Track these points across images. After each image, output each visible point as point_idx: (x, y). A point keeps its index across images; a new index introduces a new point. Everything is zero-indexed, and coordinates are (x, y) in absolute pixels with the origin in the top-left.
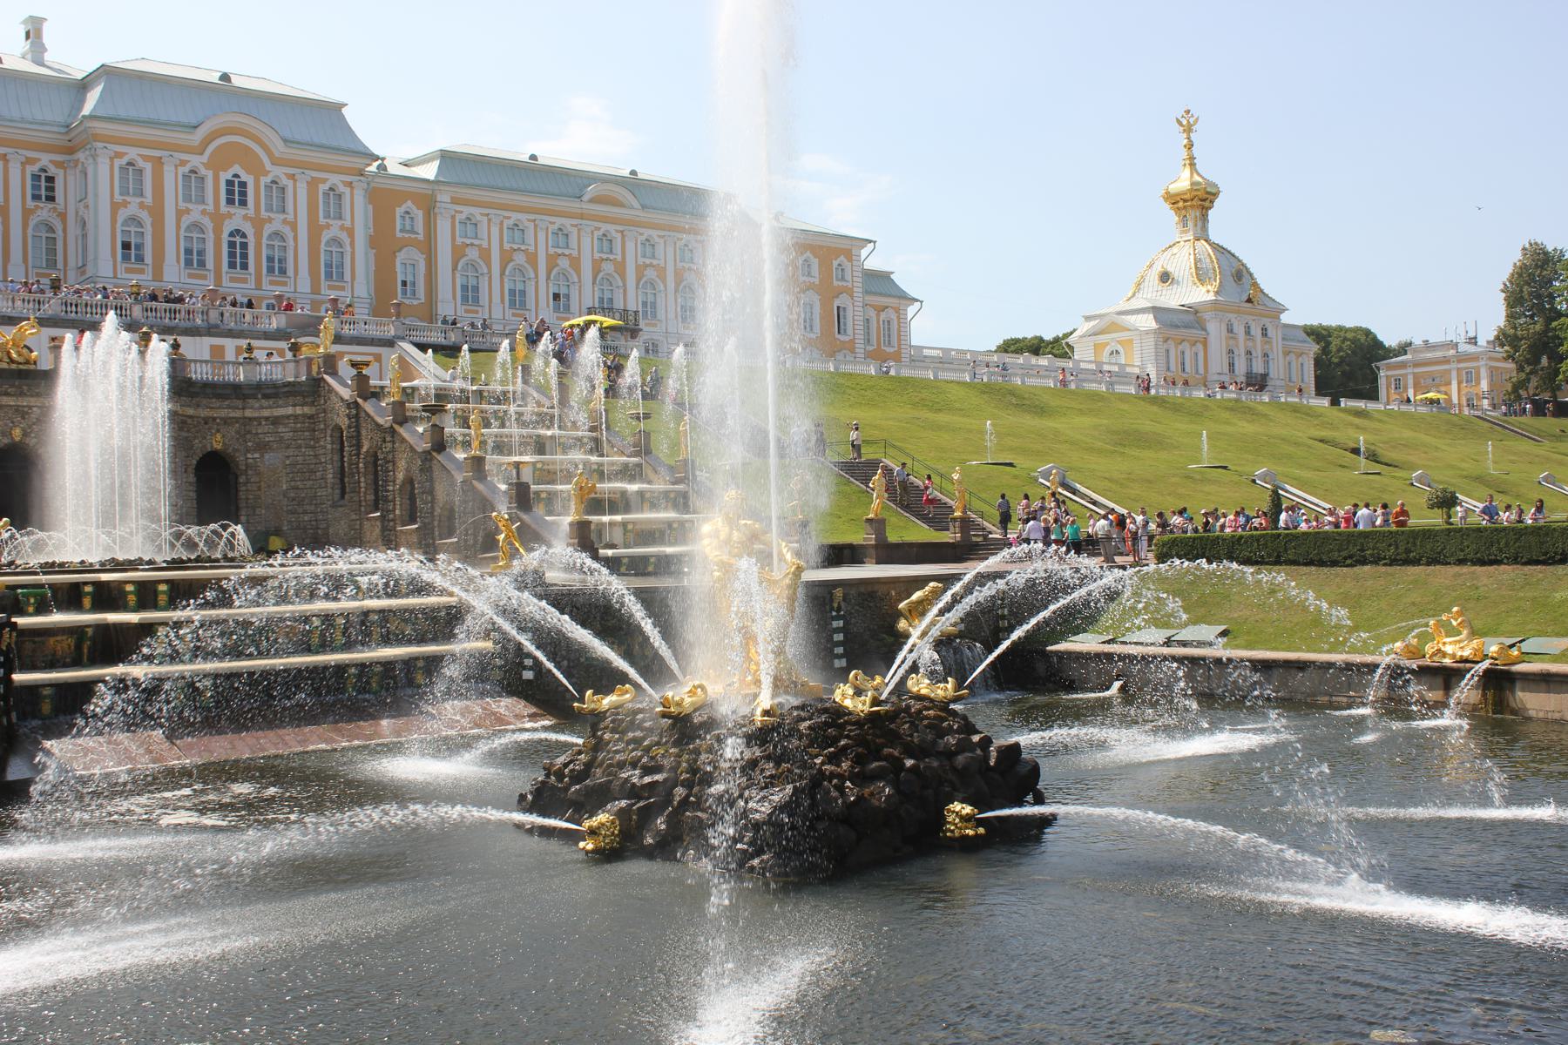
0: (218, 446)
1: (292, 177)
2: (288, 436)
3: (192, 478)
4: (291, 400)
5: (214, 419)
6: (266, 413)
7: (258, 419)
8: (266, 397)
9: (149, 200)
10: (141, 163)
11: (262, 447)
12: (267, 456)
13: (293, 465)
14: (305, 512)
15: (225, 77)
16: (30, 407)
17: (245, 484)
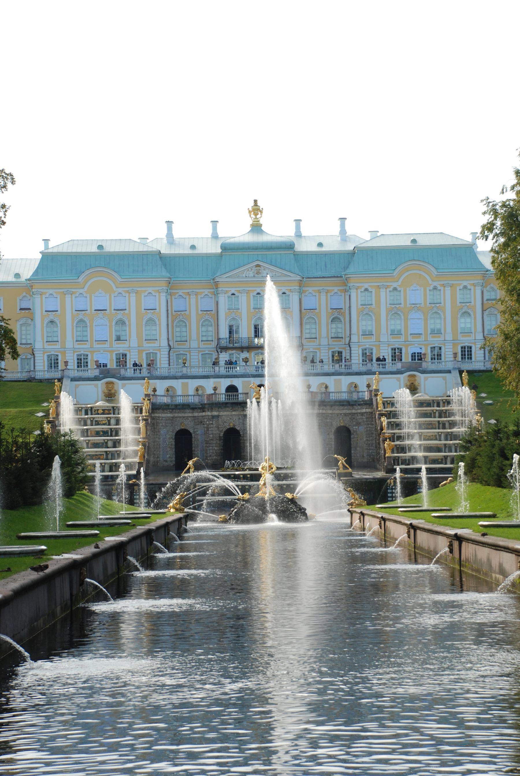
0: (342, 425)
1: (444, 286)
2: (365, 420)
3: (332, 436)
4: (365, 407)
5: (341, 414)
6: (359, 411)
7: (357, 413)
8: (359, 405)
9: (374, 306)
10: (370, 290)
11: (359, 424)
12: (360, 428)
13: (367, 431)
14: (370, 449)
15: (414, 241)
17: (353, 438)
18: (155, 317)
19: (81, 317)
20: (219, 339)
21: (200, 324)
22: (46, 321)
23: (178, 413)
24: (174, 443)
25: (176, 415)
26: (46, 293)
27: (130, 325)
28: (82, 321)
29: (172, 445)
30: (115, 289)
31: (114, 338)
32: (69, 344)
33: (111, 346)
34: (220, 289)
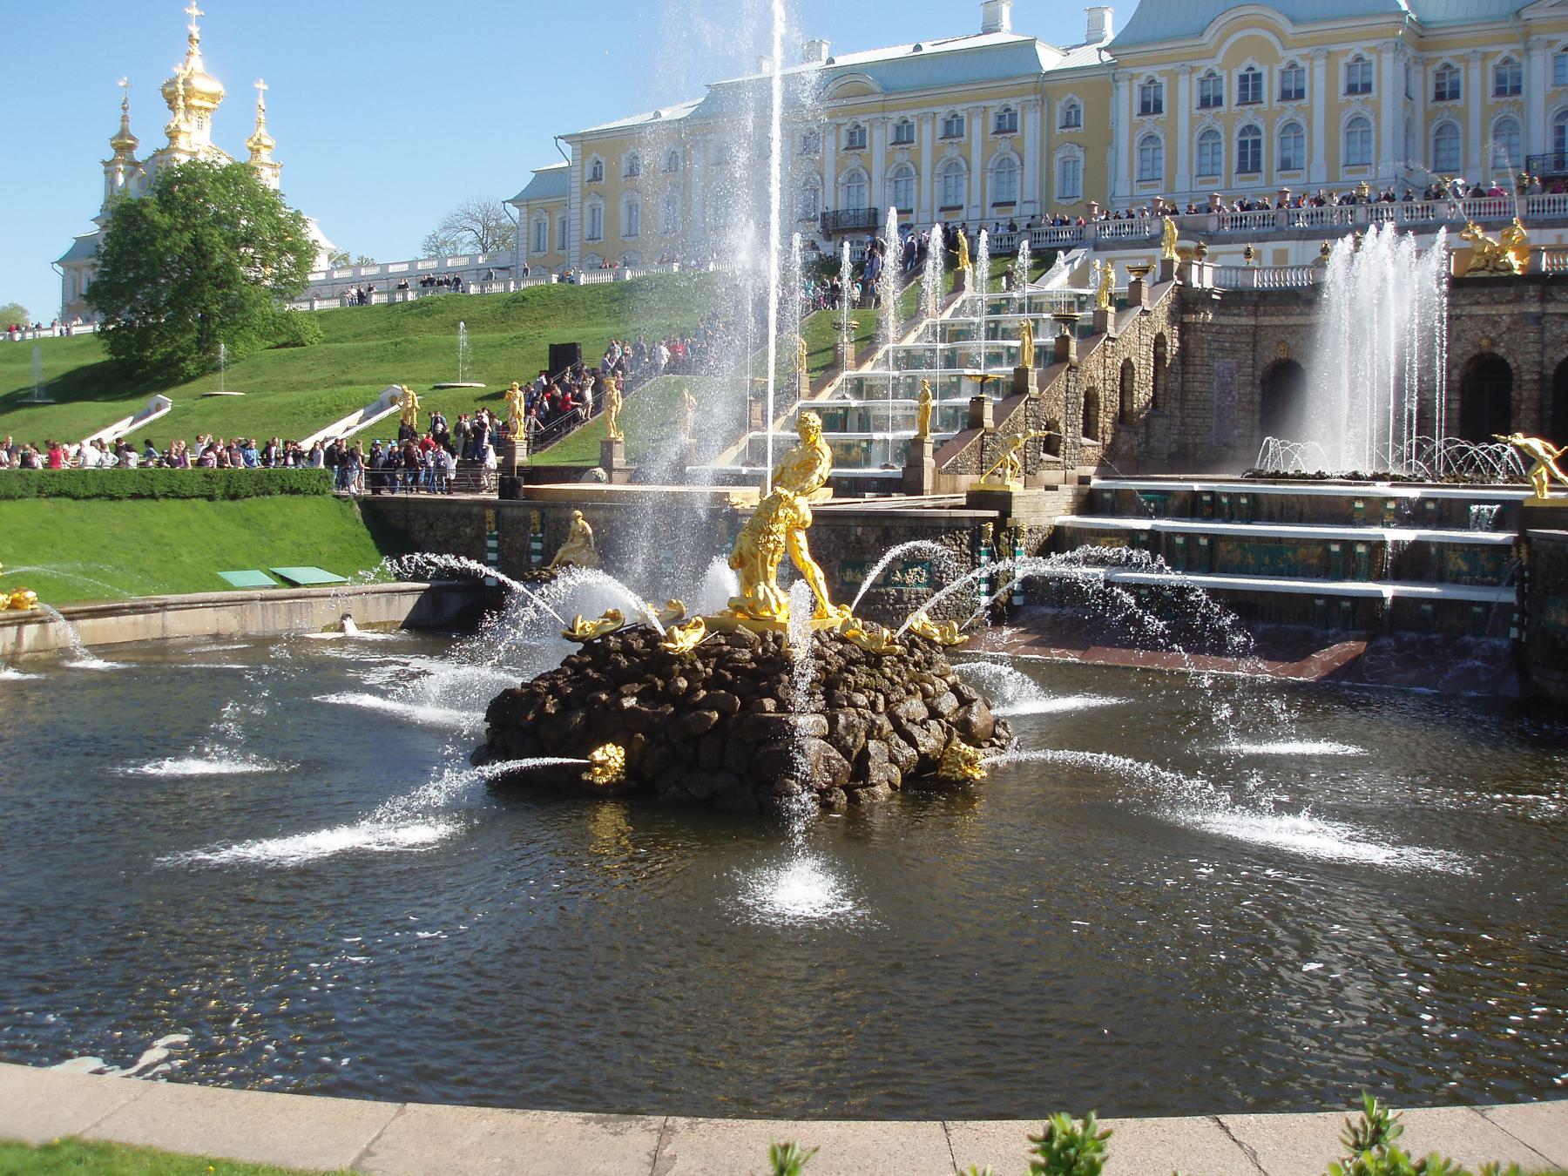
16: (1500, 316)
18: (1367, 114)
19: (1208, 121)
20: (1528, 159)
21: (1491, 128)
22: (1137, 139)
23: (1272, 314)
24: (1257, 398)
25: (1266, 321)
26: (1139, 75)
27: (1311, 132)
28: (1210, 133)
29: (1251, 402)
30: (1281, 53)
31: (1276, 164)
32: (1182, 185)
33: (1269, 183)
34: (1534, 38)
